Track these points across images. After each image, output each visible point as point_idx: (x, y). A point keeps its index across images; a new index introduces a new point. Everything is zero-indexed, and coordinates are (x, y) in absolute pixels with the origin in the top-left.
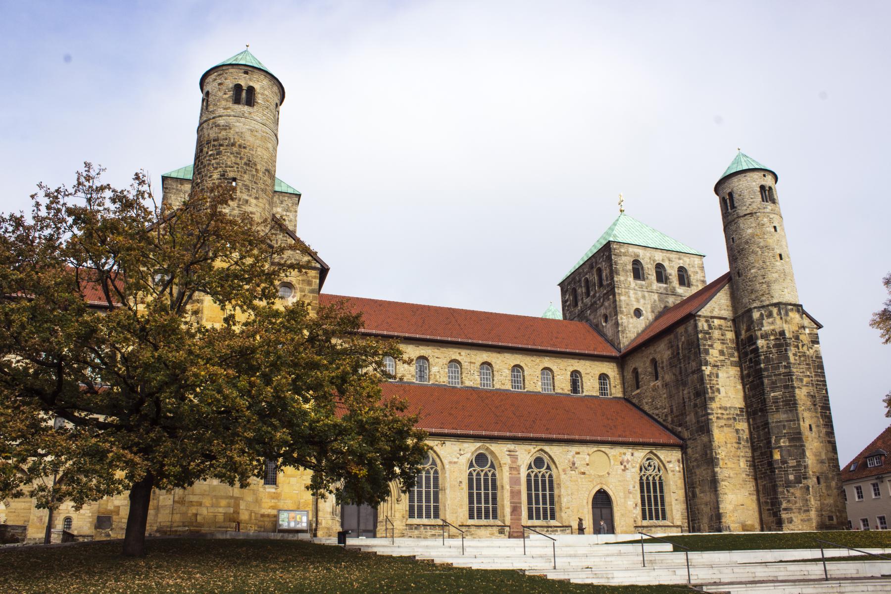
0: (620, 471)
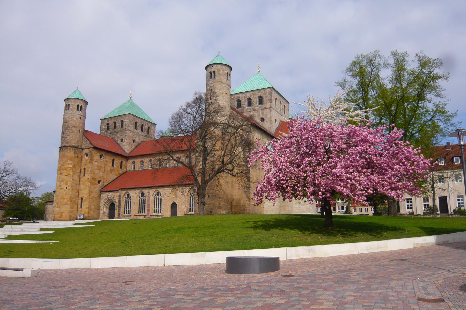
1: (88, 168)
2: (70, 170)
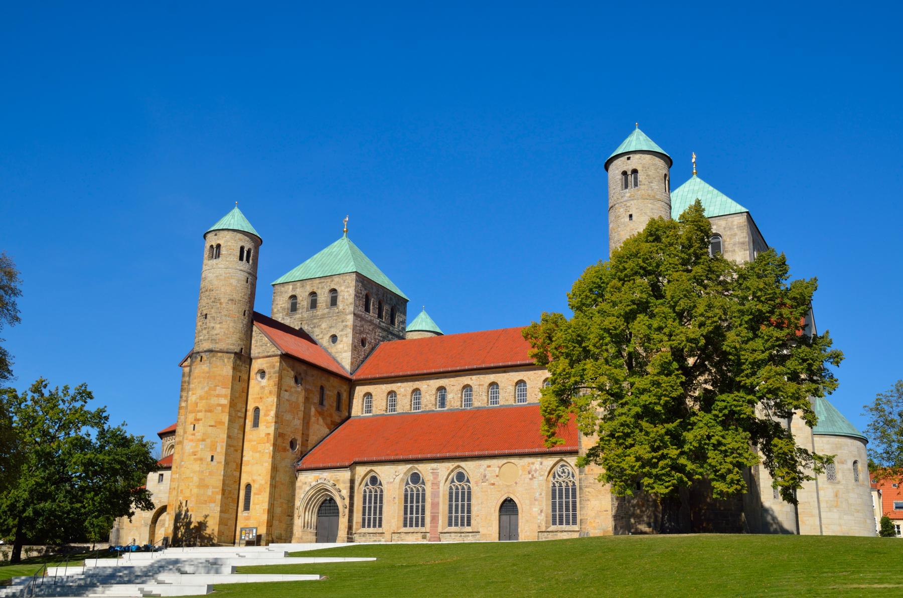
0: (527, 480)
1: (267, 407)
2: (223, 412)
